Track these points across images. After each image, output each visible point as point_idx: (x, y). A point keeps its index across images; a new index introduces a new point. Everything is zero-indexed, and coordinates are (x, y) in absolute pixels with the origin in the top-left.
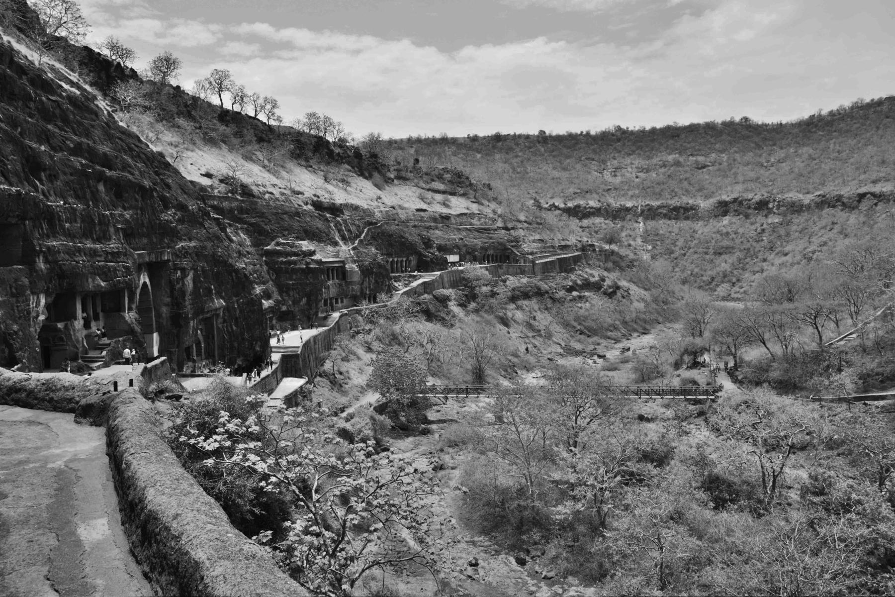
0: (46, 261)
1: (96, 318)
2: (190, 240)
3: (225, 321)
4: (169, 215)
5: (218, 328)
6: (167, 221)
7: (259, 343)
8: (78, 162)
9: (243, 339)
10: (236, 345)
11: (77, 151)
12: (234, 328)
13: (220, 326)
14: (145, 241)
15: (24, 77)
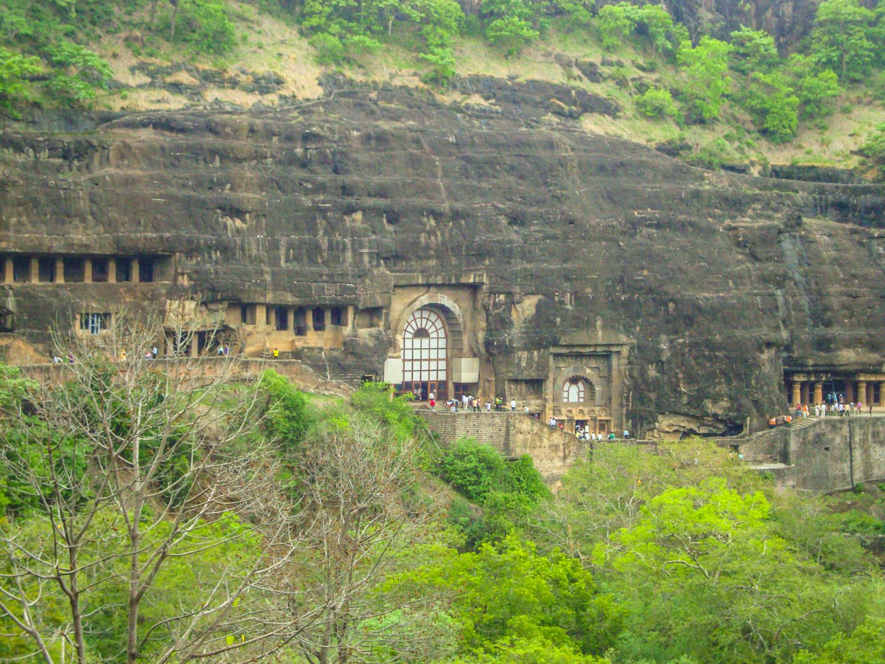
0: (190, 279)
1: (319, 327)
2: (565, 261)
3: (630, 363)
4: (514, 235)
5: (619, 371)
6: (498, 242)
7: (725, 403)
8: (306, 201)
9: (676, 391)
10: (653, 396)
11: (321, 188)
12: (652, 372)
13: (622, 368)
14: (432, 263)
15: (275, 139)
